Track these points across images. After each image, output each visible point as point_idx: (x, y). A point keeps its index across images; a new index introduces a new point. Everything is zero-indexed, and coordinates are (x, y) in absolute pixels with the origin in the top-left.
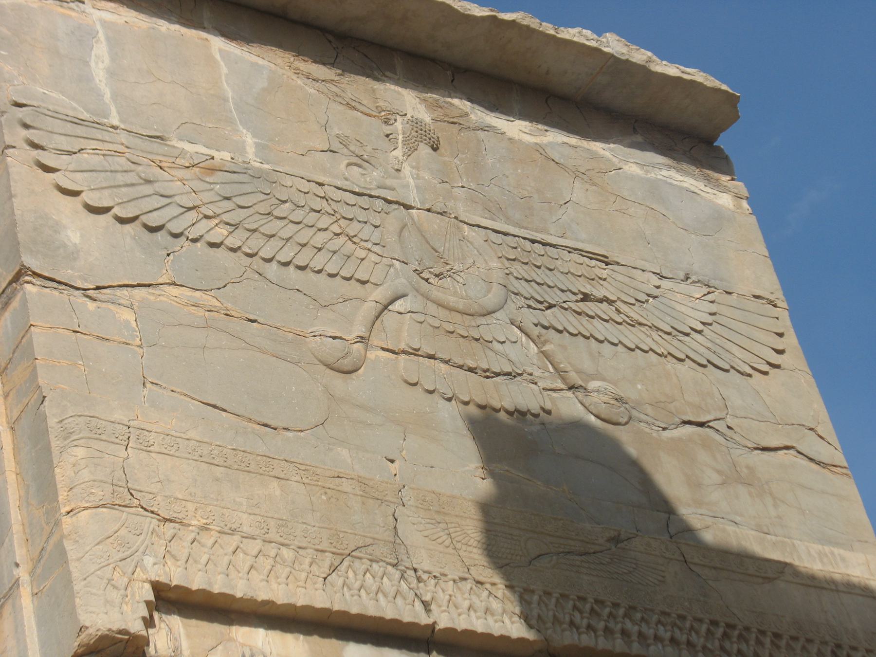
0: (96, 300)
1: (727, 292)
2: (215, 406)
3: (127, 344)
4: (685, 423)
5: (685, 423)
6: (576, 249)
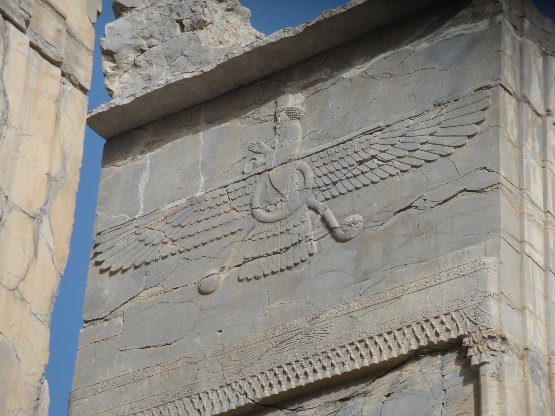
0: (109, 320)
1: (455, 101)
2: (147, 347)
3: (116, 335)
4: (396, 213)
6: (363, 133)
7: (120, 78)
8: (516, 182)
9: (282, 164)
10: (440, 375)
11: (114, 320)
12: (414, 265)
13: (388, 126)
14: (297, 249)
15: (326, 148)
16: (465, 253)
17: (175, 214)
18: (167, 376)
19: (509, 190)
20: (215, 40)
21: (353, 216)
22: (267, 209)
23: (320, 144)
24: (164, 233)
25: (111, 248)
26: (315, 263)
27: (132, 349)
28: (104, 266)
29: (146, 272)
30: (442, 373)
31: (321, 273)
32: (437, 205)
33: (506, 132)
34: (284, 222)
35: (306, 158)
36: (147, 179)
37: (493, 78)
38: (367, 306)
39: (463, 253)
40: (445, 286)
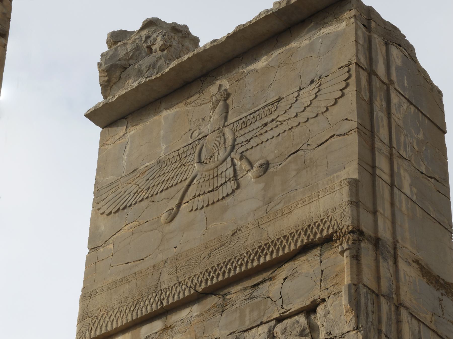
1: (326, 76)
2: (128, 263)
3: (109, 257)
5: (290, 156)
7: (111, 88)
8: (369, 127)
9: (214, 131)
10: (320, 261)
11: (107, 246)
12: (302, 190)
13: (283, 98)
14: (224, 187)
15: (243, 117)
16: (336, 178)
17: (145, 172)
18: (141, 280)
19: (363, 132)
20: (173, 57)
21: (260, 161)
22: (205, 162)
23: (239, 115)
24: (138, 186)
25: (105, 199)
26: (237, 194)
27: (119, 265)
28: (101, 211)
29: (127, 213)
30: (321, 259)
31: (241, 202)
32: (316, 147)
33: (361, 94)
34: (216, 170)
35: (230, 125)
36: (128, 151)
37: (350, 59)
38: (271, 219)
39: (334, 177)
40: (321, 201)
